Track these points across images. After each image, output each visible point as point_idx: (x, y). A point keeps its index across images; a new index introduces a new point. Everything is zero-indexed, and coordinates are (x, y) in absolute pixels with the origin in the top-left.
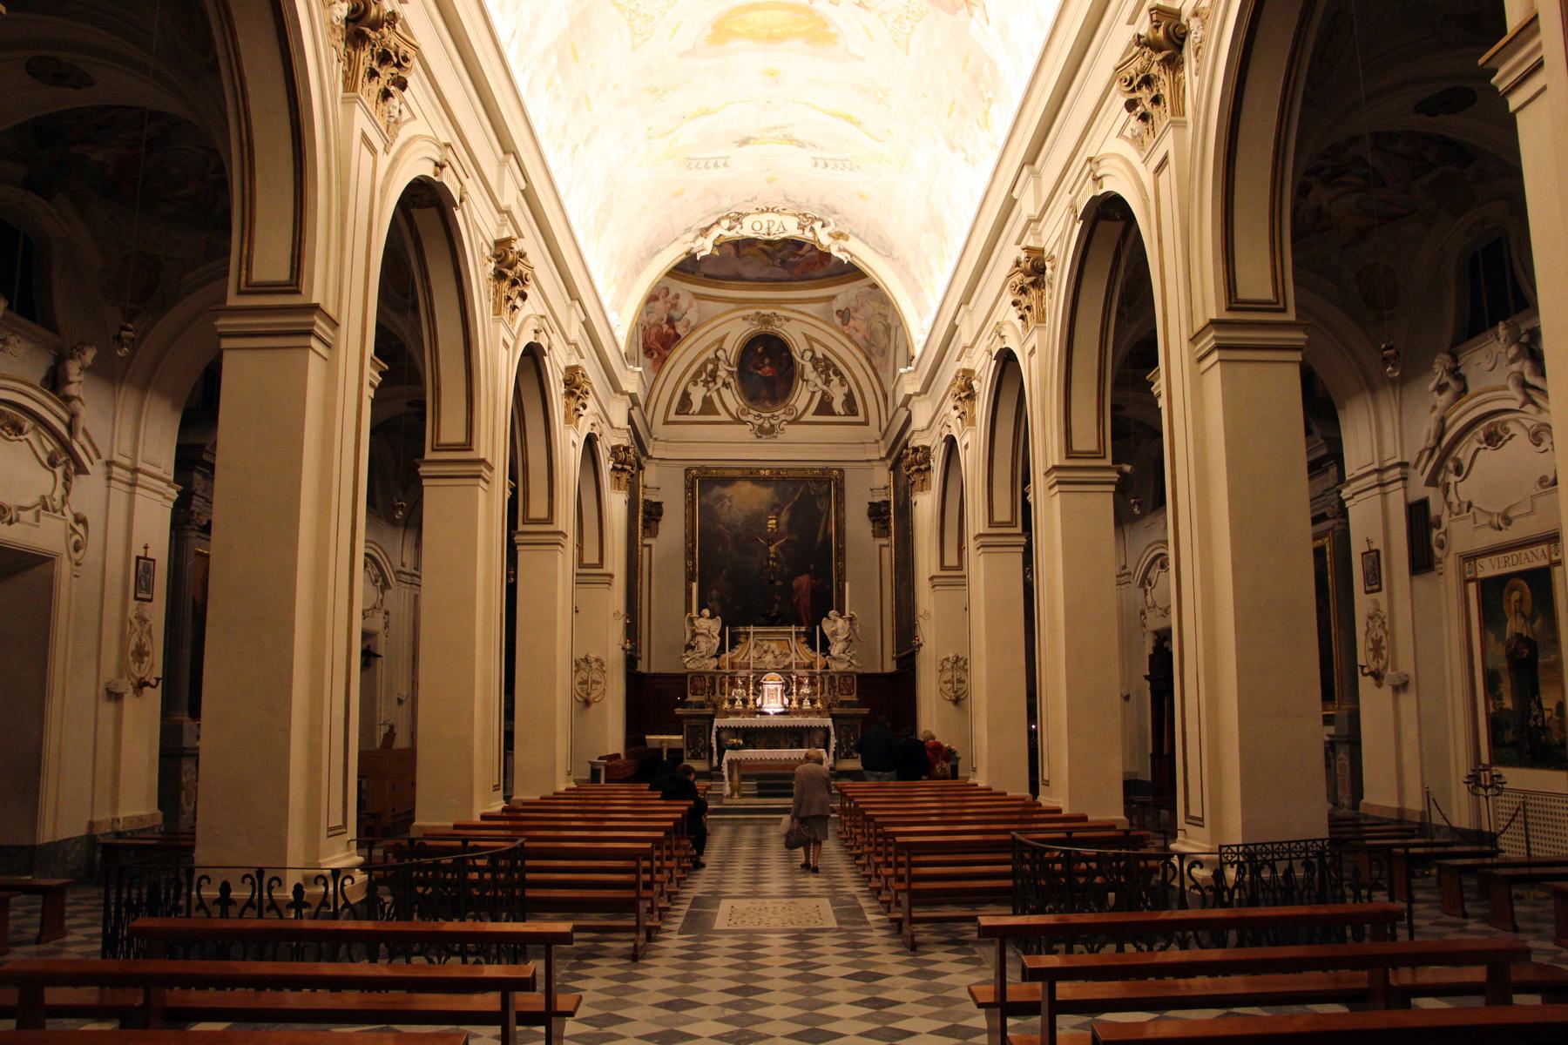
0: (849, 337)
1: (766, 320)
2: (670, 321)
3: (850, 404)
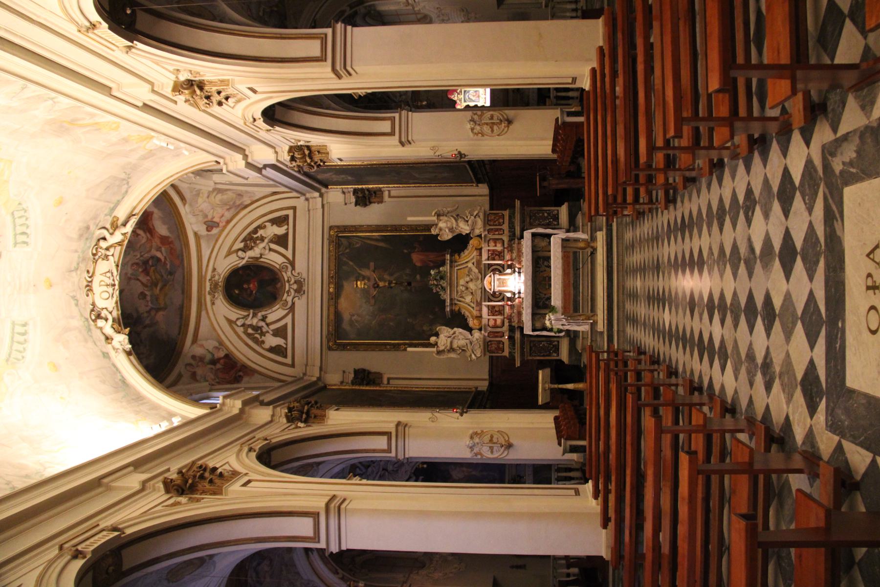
0: (228, 222)
1: (215, 286)
2: (214, 362)
3: (280, 221)
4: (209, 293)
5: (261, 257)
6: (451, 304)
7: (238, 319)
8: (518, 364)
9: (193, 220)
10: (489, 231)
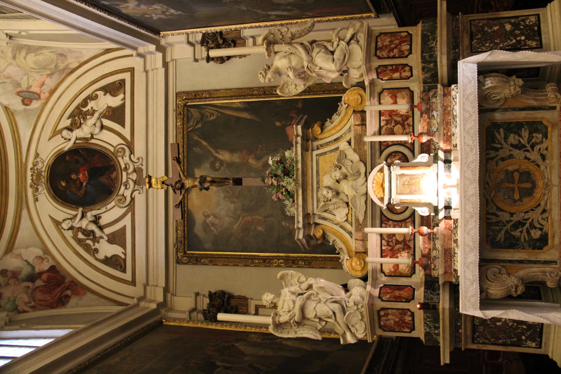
0: (52, 92)
2: (32, 278)
3: (113, 89)
4: (31, 186)
6: (307, 225)
7: (64, 220)
8: (445, 358)
10: (380, 71)
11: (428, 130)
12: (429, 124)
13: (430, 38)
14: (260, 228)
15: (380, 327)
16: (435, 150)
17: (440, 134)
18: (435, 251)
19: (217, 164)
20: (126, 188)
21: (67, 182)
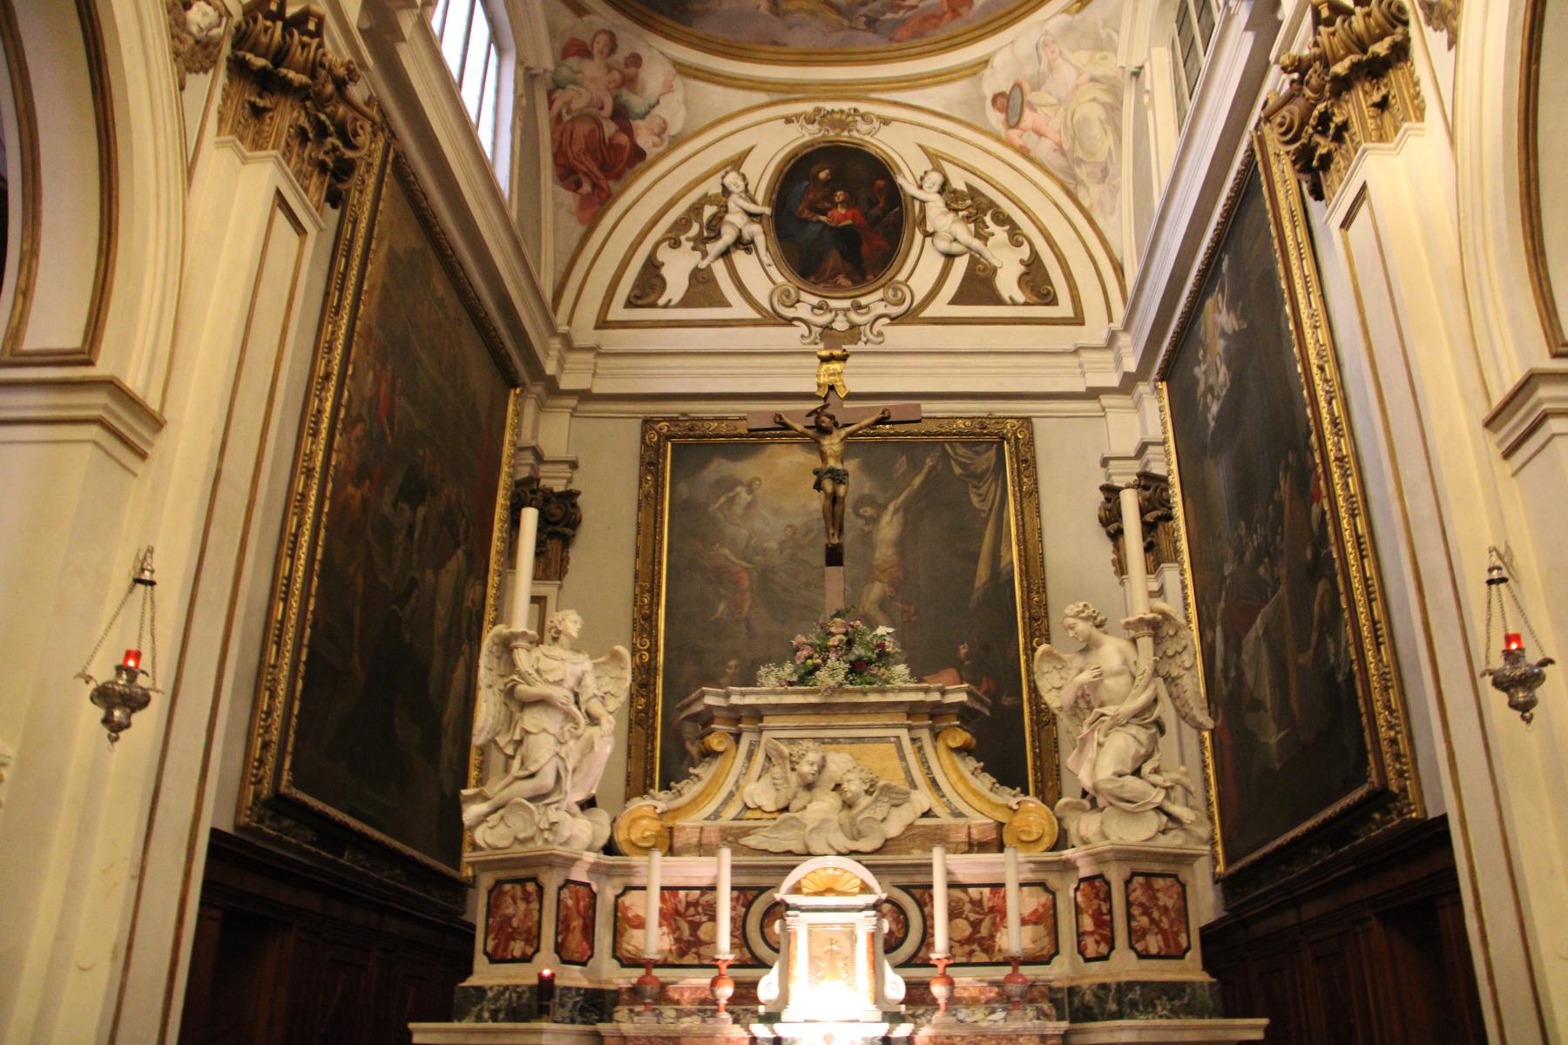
0: (1024, 152)
2: (621, 115)
3: (1035, 280)
4: (818, 110)
5: (927, 234)
6: (736, 715)
9: (1025, 47)
10: (1096, 885)
11: (959, 1000)
12: (973, 1002)
13: (1177, 1003)
14: (722, 607)
15: (499, 883)
16: (913, 1016)
17: (950, 1027)
18: (673, 1014)
19: (868, 511)
20: (814, 307)
21: (826, 183)
